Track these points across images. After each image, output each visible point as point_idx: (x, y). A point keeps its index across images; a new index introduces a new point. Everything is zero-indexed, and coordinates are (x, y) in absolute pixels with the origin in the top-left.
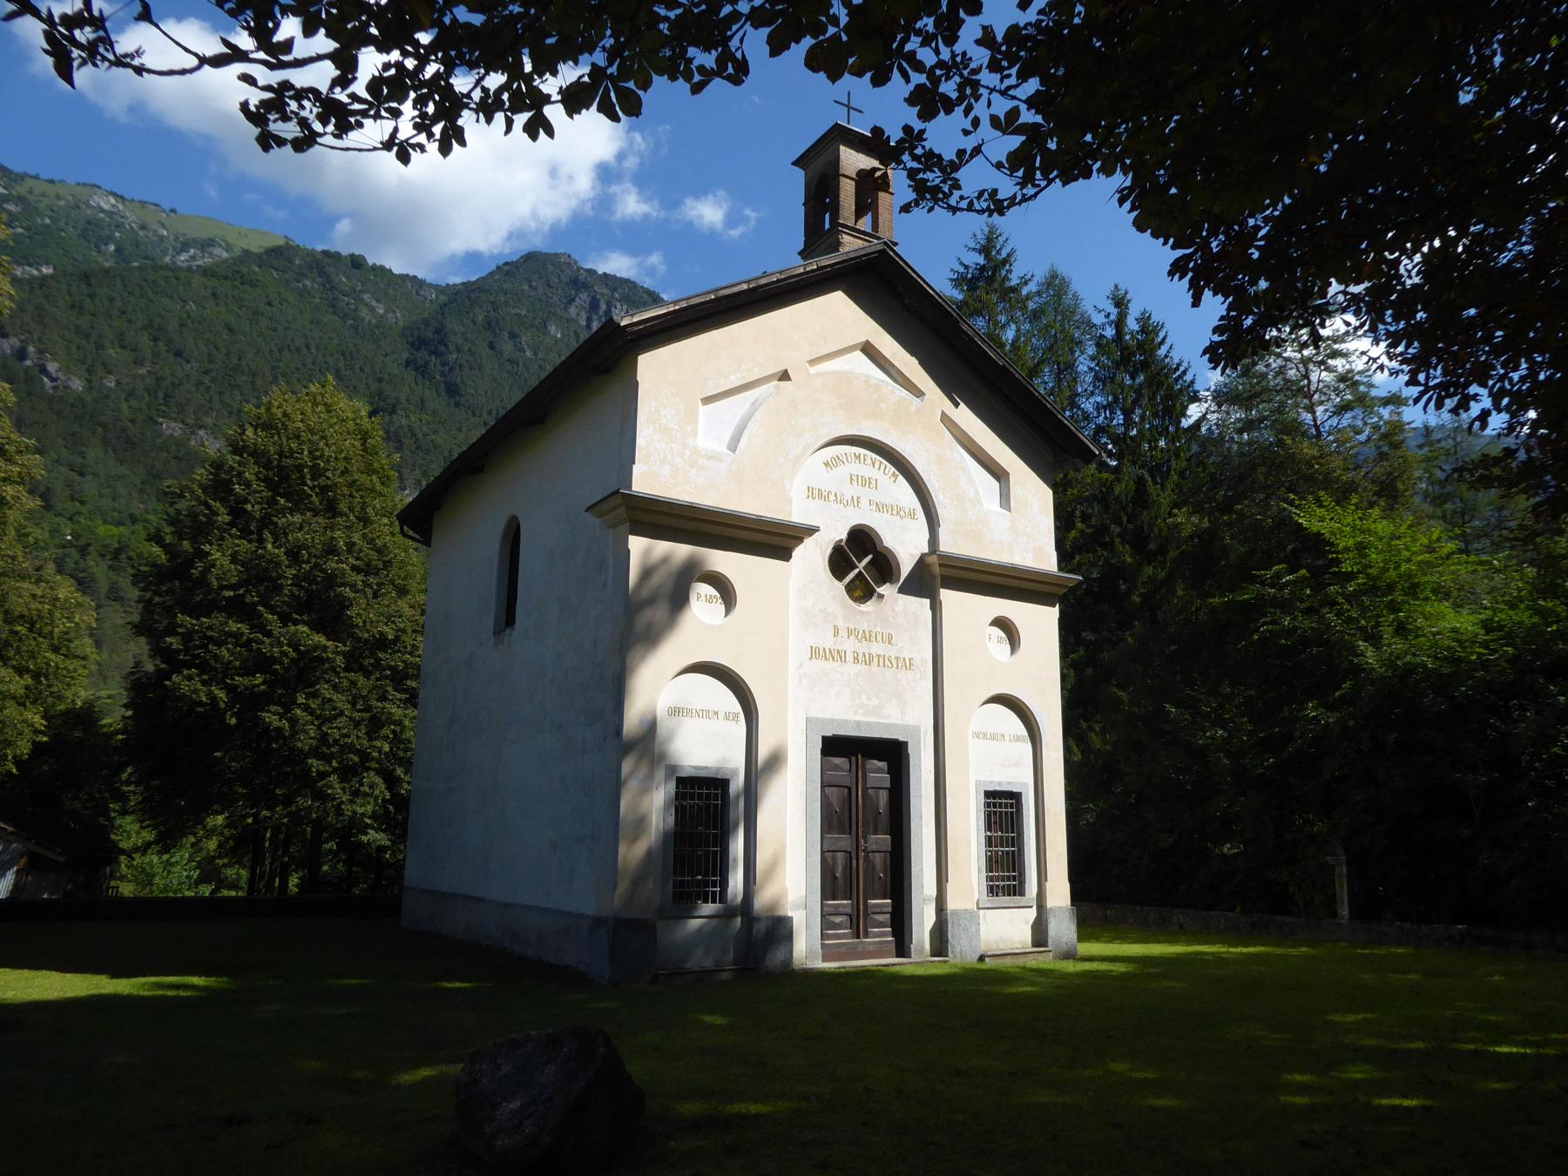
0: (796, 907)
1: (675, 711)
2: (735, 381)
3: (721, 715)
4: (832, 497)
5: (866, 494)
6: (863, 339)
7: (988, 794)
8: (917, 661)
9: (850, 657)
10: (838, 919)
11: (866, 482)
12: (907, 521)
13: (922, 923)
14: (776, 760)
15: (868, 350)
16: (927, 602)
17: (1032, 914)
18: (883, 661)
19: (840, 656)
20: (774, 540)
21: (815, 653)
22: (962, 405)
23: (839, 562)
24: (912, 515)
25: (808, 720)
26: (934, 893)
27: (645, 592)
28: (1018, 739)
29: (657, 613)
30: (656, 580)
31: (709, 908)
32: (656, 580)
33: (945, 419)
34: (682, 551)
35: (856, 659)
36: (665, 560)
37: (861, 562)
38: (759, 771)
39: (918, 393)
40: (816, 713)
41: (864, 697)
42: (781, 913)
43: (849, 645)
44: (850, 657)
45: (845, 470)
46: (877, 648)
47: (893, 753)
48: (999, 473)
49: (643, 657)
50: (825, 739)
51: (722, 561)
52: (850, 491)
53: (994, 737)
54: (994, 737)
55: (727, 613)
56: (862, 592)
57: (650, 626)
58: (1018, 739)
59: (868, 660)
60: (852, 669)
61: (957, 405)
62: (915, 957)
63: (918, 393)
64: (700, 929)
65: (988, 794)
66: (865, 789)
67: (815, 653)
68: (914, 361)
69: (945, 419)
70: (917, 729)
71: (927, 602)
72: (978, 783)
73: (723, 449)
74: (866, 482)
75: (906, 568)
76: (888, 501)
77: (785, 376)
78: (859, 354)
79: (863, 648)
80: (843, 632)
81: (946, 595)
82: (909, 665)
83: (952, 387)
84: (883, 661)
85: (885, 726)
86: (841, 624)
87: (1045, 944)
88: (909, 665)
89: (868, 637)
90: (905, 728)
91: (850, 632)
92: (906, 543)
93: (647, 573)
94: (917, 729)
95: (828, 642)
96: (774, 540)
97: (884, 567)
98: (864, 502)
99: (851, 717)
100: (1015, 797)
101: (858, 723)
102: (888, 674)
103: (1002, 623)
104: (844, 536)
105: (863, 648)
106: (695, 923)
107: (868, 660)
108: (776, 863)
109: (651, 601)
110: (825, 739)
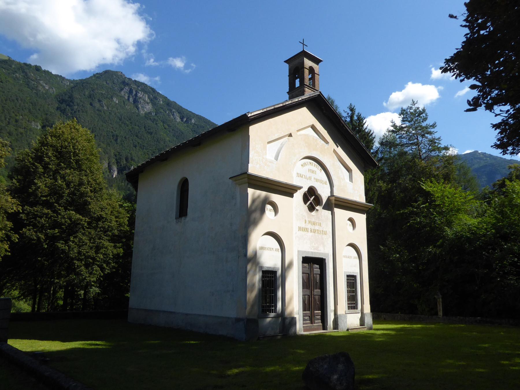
1: (262, 248)
3: (274, 250)
5: (313, 176)
7: (348, 276)
11: (313, 172)
14: (291, 264)
15: (313, 127)
17: (359, 315)
19: (306, 230)
20: (288, 190)
21: (300, 229)
23: (306, 198)
24: (326, 183)
27: (253, 208)
28: (355, 258)
29: (256, 215)
30: (256, 203)
31: (272, 315)
32: (256, 203)
33: (335, 151)
34: (263, 194)
36: (259, 197)
37: (312, 199)
38: (285, 268)
39: (327, 142)
40: (300, 249)
42: (293, 316)
43: (309, 226)
44: (309, 231)
46: (317, 227)
47: (321, 262)
48: (349, 170)
50: (303, 258)
51: (275, 198)
52: (309, 174)
55: (275, 215)
57: (255, 219)
58: (355, 258)
59: (314, 231)
60: (310, 234)
61: (338, 147)
62: (328, 330)
63: (327, 142)
64: (270, 322)
65: (348, 276)
66: (313, 274)
67: (300, 229)
68: (326, 132)
69: (335, 151)
72: (345, 272)
73: (273, 159)
74: (313, 172)
75: (324, 201)
77: (290, 135)
78: (310, 128)
79: (313, 227)
80: (307, 222)
81: (336, 210)
82: (325, 233)
83: (337, 141)
85: (320, 253)
87: (364, 325)
88: (325, 233)
89: (314, 224)
92: (324, 193)
93: (254, 201)
94: (328, 254)
95: (303, 225)
96: (288, 190)
97: (318, 200)
98: (313, 178)
100: (354, 277)
101: (312, 252)
103: (351, 220)
105: (313, 227)
106: (268, 320)
107: (314, 231)
108: (291, 299)
109: (255, 211)
110: (303, 258)
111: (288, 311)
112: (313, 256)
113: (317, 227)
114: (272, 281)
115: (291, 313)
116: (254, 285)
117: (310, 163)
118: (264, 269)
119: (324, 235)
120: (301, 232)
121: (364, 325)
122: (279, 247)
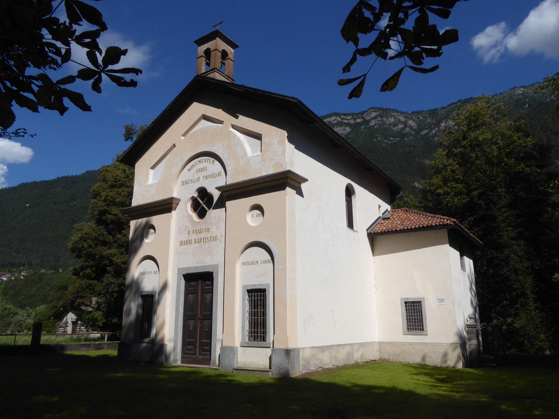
0: (170, 341)
1: (143, 274)
2: (159, 157)
4: (190, 182)
5: (201, 175)
6: (201, 115)
8: (219, 237)
11: (202, 170)
12: (218, 178)
18: (205, 240)
21: (182, 243)
22: (241, 117)
25: (179, 269)
27: (135, 237)
28: (265, 262)
29: (138, 242)
30: (138, 232)
31: (147, 340)
33: (234, 127)
41: (197, 257)
43: (193, 237)
45: (194, 169)
46: (203, 235)
48: (258, 137)
49: (133, 258)
51: (156, 220)
53: (253, 263)
54: (253, 263)
58: (265, 262)
60: (194, 246)
61: (237, 117)
63: (221, 122)
70: (217, 266)
72: (244, 286)
74: (202, 170)
76: (210, 174)
78: (203, 120)
79: (198, 236)
80: (191, 233)
84: (205, 240)
86: (191, 229)
88: (215, 239)
89: (200, 232)
90: (213, 266)
94: (217, 266)
95: (185, 237)
99: (192, 265)
101: (195, 267)
102: (207, 245)
104: (196, 195)
105: (198, 236)
107: (199, 241)
111: (159, 337)
113: (203, 235)
114: (150, 303)
115: (163, 339)
116: (129, 311)
117: (199, 161)
118: (144, 294)
119: (212, 243)
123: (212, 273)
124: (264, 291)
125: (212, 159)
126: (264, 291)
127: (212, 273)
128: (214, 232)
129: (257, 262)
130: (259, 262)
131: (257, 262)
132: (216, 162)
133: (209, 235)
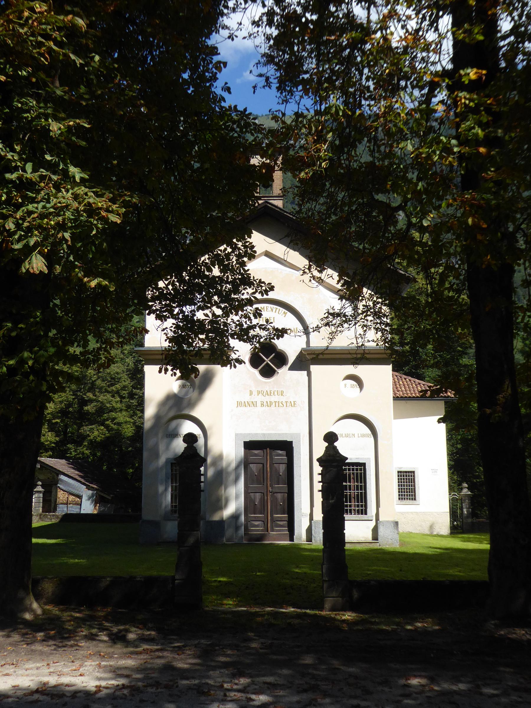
6: (264, 250)
9: (259, 404)
10: (256, 523)
13: (300, 526)
16: (305, 373)
17: (373, 524)
18: (278, 404)
19: (254, 404)
21: (239, 404)
25: (236, 435)
26: (309, 512)
35: (262, 405)
43: (259, 399)
44: (259, 404)
46: (273, 399)
50: (245, 443)
56: (268, 373)
58: (363, 436)
60: (259, 409)
66: (272, 464)
67: (239, 404)
70: (298, 435)
71: (305, 373)
75: (292, 358)
79: (267, 399)
80: (255, 393)
81: (313, 368)
82: (294, 404)
84: (278, 404)
85: (279, 434)
88: (294, 404)
89: (269, 394)
91: (259, 393)
94: (298, 435)
95: (247, 398)
97: (281, 359)
99: (260, 431)
102: (281, 410)
105: (267, 399)
112: (266, 439)
113: (273, 399)
119: (290, 408)
120: (244, 408)
121: (377, 540)
122: (370, 432)
123: (291, 442)
124: (364, 465)
125: (282, 310)
126: (364, 465)
127: (291, 442)
128: (290, 396)
129: (354, 435)
130: (356, 435)
131: (354, 435)
132: (290, 315)
133: (283, 399)
